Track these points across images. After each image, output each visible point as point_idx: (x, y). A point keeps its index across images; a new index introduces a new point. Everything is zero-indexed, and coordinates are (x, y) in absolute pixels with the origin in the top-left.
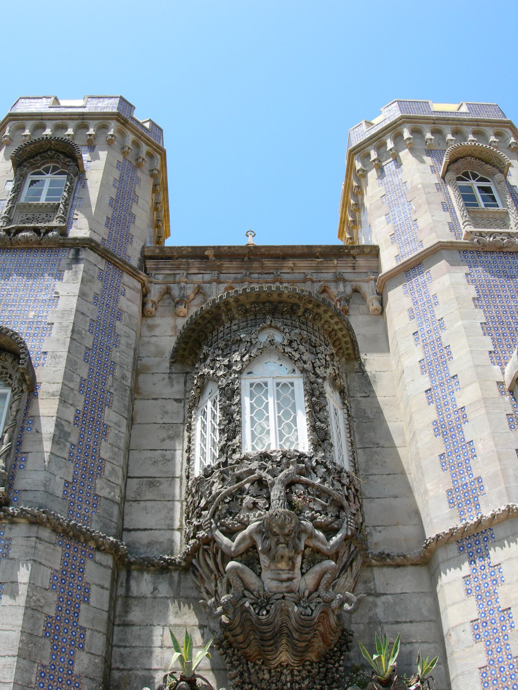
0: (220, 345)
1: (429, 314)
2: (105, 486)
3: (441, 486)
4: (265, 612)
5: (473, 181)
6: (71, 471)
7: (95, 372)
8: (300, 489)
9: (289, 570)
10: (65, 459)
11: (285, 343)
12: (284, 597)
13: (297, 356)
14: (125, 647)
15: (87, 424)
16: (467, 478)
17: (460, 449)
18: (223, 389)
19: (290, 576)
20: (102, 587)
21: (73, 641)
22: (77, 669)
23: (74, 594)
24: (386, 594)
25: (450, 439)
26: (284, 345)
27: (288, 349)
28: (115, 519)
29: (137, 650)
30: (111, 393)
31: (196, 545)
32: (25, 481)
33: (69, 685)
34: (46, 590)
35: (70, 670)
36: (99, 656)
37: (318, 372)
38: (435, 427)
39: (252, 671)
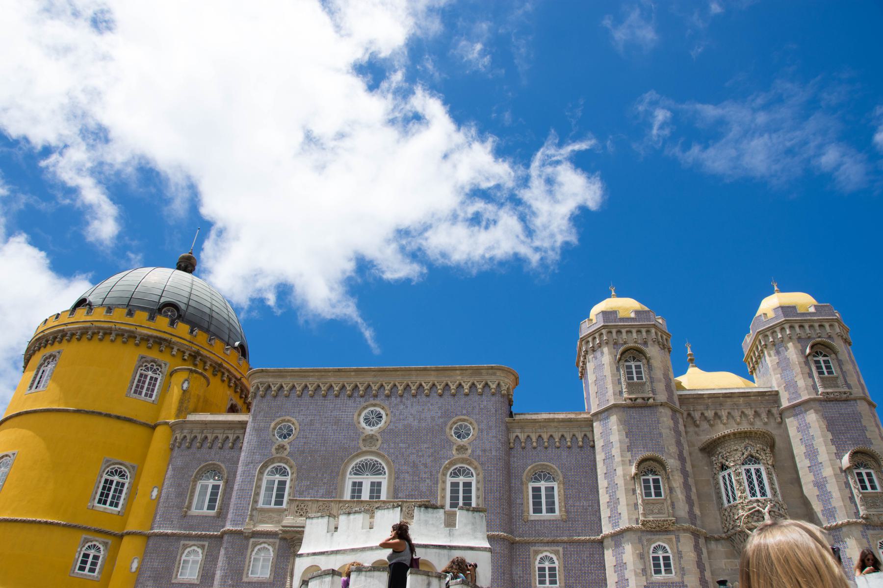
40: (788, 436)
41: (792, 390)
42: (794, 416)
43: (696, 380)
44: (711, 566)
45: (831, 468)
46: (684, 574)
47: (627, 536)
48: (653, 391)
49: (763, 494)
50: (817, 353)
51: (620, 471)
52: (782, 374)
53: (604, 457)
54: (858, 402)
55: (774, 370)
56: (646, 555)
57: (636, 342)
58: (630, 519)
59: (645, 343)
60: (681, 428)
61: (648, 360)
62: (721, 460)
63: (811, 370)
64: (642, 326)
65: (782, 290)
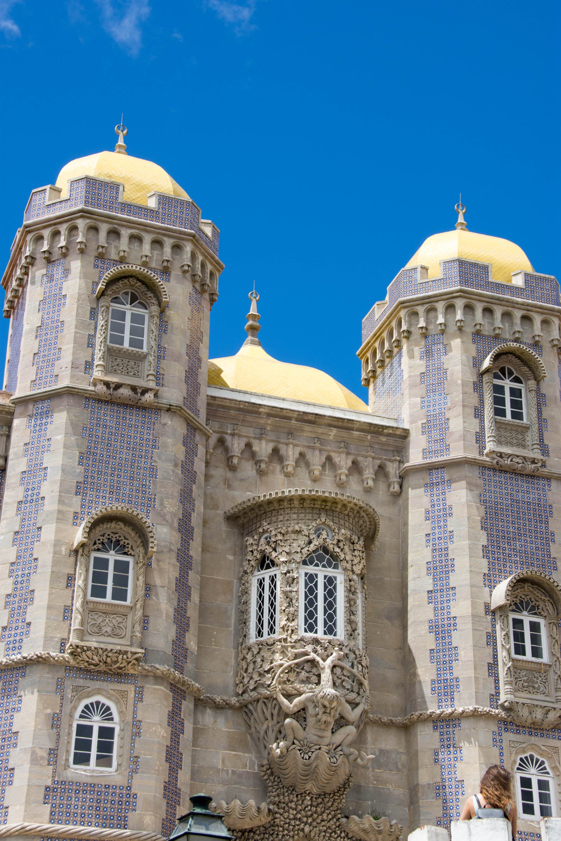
0: (282, 531)
1: (442, 522)
3: (427, 674)
4: (308, 758)
5: (507, 381)
8: (338, 671)
11: (335, 542)
12: (320, 749)
13: (342, 556)
16: (448, 675)
17: (447, 650)
18: (286, 574)
25: (441, 639)
26: (334, 544)
27: (337, 550)
31: (257, 697)
38: (430, 625)
39: (286, 794)
40: (406, 524)
41: (435, 435)
42: (426, 485)
43: (252, 372)
44: (194, 761)
45: (468, 603)
46: (135, 771)
47: (36, 674)
48: (159, 377)
49: (330, 630)
50: (502, 370)
51: (49, 533)
52: (424, 395)
53: (21, 498)
54: (554, 484)
55: (412, 386)
56: (65, 720)
57: (145, 264)
58: (47, 639)
59: (166, 271)
60: (199, 466)
61: (163, 309)
62: (263, 545)
63: (482, 402)
64: (168, 233)
65: (473, 226)
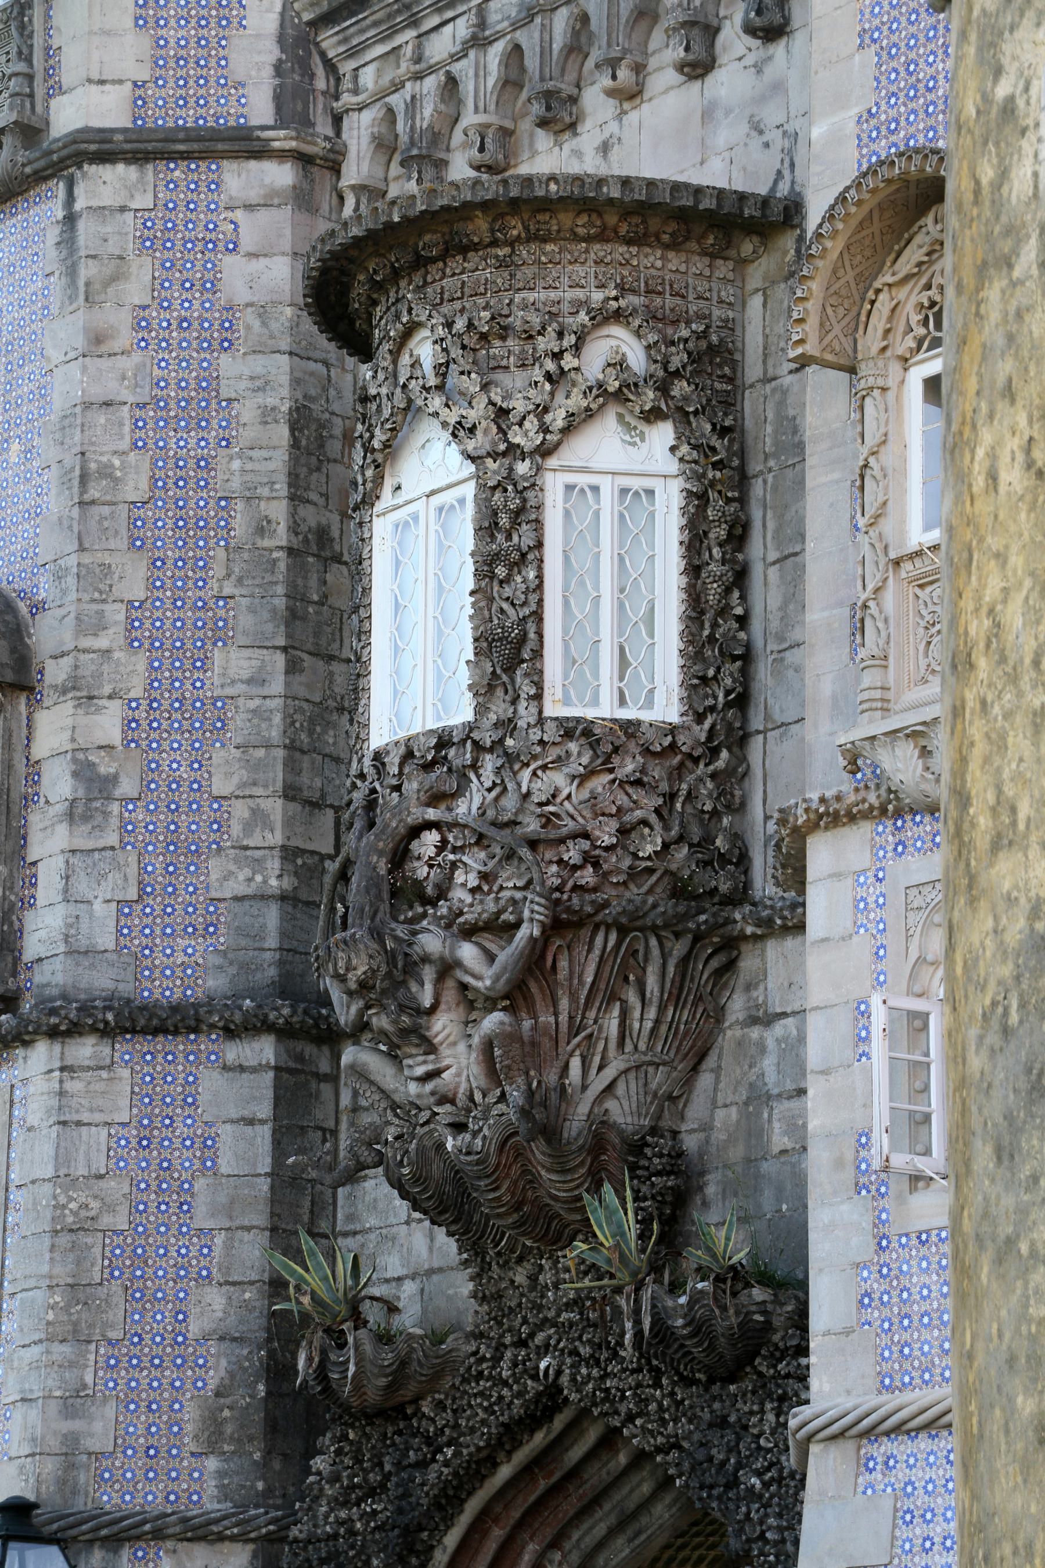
2: (233, 867)
6: (132, 871)
7: (169, 563)
9: (426, 1053)
10: (113, 848)
14: (355, 1233)
15: (165, 724)
19: (430, 1067)
20: (251, 1122)
21: (182, 1268)
22: (194, 1329)
23: (176, 1163)
24: (784, 1015)
28: (272, 941)
29: (372, 1236)
30: (225, 598)
32: (38, 935)
33: (178, 1367)
34: (101, 1177)
35: (180, 1334)
36: (252, 1283)
37: (517, 440)
